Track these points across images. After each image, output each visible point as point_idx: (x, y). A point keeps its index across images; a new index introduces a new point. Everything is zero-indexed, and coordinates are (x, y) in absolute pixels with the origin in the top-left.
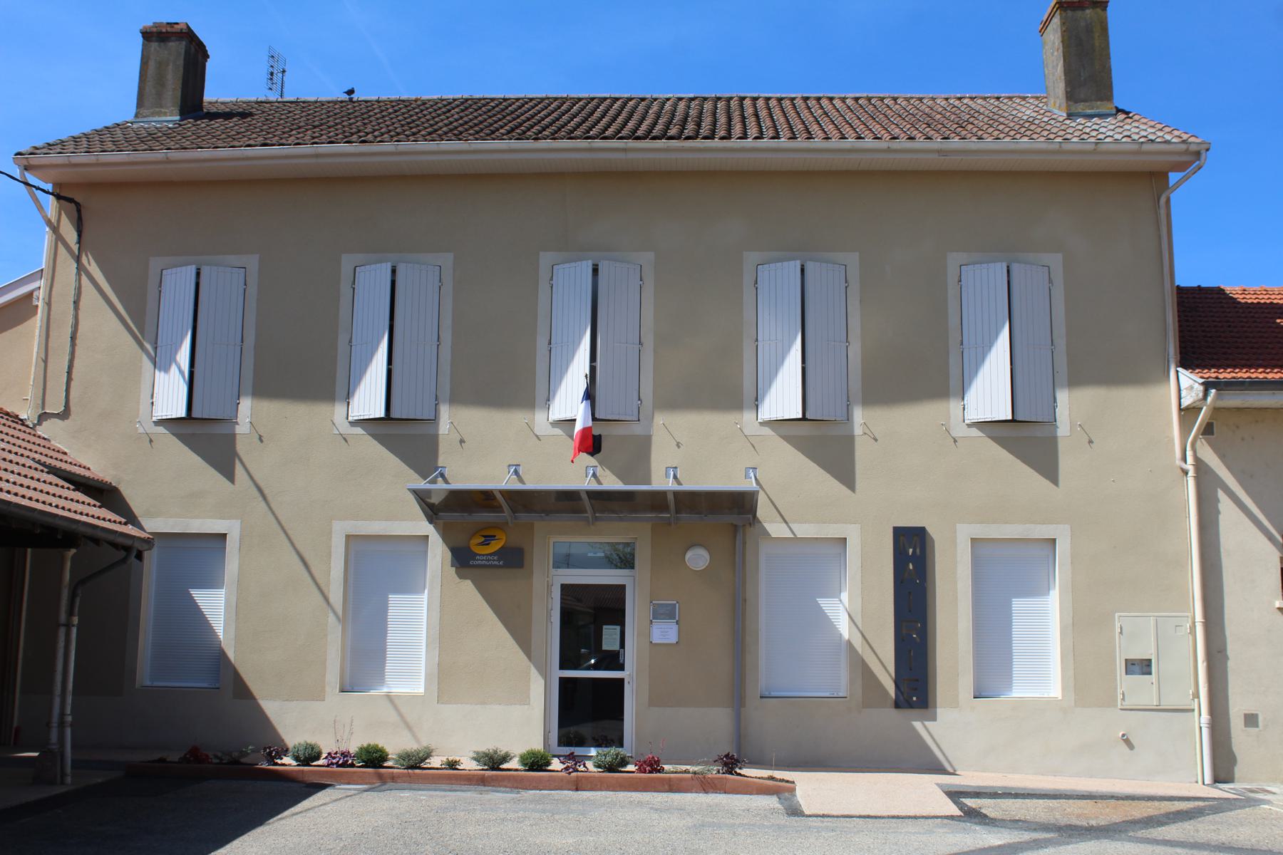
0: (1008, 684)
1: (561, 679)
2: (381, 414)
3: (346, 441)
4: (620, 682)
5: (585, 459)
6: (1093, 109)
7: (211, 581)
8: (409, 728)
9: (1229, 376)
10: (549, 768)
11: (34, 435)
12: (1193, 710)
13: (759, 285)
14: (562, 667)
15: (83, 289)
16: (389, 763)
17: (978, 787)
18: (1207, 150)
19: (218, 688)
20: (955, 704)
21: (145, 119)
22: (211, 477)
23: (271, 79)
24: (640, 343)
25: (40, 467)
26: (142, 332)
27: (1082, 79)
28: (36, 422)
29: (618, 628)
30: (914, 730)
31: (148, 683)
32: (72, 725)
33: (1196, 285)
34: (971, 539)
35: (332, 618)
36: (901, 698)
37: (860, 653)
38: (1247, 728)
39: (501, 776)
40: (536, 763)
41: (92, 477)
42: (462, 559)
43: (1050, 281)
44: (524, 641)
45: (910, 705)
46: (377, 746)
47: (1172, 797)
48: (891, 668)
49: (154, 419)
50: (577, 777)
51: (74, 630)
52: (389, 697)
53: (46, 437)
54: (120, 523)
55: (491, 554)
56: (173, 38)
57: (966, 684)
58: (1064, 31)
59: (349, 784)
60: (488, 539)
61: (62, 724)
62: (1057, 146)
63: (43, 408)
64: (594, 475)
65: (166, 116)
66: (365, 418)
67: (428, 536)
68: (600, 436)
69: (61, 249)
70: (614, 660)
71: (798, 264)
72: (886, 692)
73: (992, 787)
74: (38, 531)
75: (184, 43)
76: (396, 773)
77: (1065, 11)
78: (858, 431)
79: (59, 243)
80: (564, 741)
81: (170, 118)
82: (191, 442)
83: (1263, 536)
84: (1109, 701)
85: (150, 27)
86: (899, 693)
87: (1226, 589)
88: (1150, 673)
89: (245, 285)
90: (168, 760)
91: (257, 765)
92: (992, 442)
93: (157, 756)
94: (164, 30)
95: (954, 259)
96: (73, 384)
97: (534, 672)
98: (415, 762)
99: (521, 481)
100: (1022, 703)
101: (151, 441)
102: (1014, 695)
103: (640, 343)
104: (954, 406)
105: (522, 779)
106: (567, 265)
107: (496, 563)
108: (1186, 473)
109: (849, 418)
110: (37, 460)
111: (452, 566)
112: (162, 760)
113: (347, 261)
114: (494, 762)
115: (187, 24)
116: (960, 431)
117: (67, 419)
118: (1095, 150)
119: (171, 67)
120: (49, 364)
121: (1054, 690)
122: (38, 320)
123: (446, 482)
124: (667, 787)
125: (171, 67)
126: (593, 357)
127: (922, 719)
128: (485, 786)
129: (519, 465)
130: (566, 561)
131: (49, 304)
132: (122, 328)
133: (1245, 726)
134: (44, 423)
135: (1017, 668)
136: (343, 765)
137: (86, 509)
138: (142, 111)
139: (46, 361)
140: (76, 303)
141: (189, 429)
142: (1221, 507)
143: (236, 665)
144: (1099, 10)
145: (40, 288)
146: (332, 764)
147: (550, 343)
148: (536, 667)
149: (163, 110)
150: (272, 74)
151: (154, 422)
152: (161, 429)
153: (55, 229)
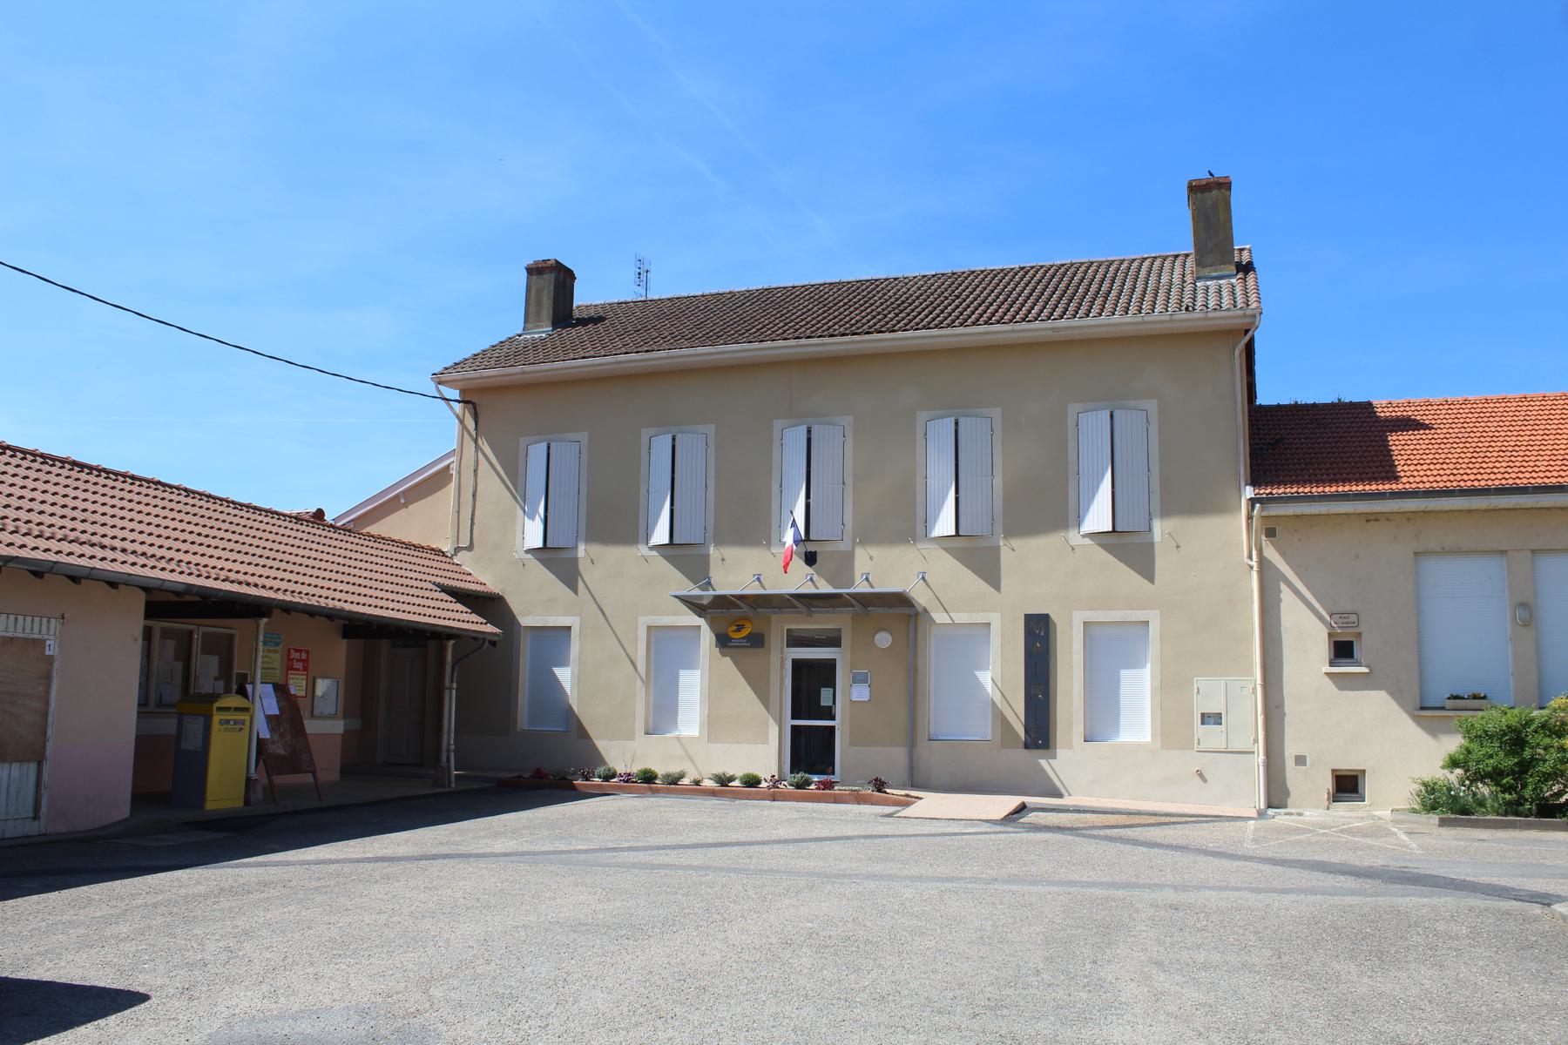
0: (1117, 734)
1: (792, 726)
2: (667, 541)
4: (833, 728)
7: (563, 663)
8: (691, 760)
10: (760, 786)
12: (1254, 752)
14: (793, 718)
16: (657, 782)
17: (1057, 805)
18: (1261, 313)
20: (1070, 746)
22: (561, 589)
24: (844, 483)
25: (435, 588)
26: (517, 492)
29: (832, 690)
30: (1039, 764)
31: (526, 728)
34: (1084, 623)
35: (639, 683)
36: (1029, 741)
37: (1000, 706)
41: (486, 591)
42: (723, 641)
43: (1148, 422)
44: (765, 701)
45: (1037, 747)
51: (454, 692)
52: (678, 738)
54: (481, 623)
57: (1078, 731)
61: (448, 750)
62: (1140, 319)
64: (811, 579)
65: (543, 327)
68: (816, 552)
70: (829, 713)
71: (953, 419)
72: (1018, 735)
73: (1067, 805)
75: (553, 274)
81: (543, 331)
82: (546, 563)
84: (1187, 743)
86: (1028, 738)
87: (1284, 659)
88: (1221, 724)
93: (516, 775)
95: (1073, 408)
96: (475, 526)
97: (771, 720)
98: (674, 780)
99: (763, 586)
101: (524, 565)
103: (844, 483)
105: (739, 792)
106: (791, 429)
108: (1252, 567)
112: (520, 777)
113: (645, 433)
114: (724, 781)
115: (556, 261)
119: (546, 292)
121: (1146, 737)
122: (453, 486)
125: (546, 292)
126: (808, 496)
127: (1047, 758)
130: (795, 640)
131: (459, 473)
133: (1296, 764)
134: (459, 554)
136: (627, 782)
138: (530, 326)
139: (458, 512)
142: (1282, 596)
147: (781, 486)
150: (640, 274)
152: (529, 556)
153: (461, 422)
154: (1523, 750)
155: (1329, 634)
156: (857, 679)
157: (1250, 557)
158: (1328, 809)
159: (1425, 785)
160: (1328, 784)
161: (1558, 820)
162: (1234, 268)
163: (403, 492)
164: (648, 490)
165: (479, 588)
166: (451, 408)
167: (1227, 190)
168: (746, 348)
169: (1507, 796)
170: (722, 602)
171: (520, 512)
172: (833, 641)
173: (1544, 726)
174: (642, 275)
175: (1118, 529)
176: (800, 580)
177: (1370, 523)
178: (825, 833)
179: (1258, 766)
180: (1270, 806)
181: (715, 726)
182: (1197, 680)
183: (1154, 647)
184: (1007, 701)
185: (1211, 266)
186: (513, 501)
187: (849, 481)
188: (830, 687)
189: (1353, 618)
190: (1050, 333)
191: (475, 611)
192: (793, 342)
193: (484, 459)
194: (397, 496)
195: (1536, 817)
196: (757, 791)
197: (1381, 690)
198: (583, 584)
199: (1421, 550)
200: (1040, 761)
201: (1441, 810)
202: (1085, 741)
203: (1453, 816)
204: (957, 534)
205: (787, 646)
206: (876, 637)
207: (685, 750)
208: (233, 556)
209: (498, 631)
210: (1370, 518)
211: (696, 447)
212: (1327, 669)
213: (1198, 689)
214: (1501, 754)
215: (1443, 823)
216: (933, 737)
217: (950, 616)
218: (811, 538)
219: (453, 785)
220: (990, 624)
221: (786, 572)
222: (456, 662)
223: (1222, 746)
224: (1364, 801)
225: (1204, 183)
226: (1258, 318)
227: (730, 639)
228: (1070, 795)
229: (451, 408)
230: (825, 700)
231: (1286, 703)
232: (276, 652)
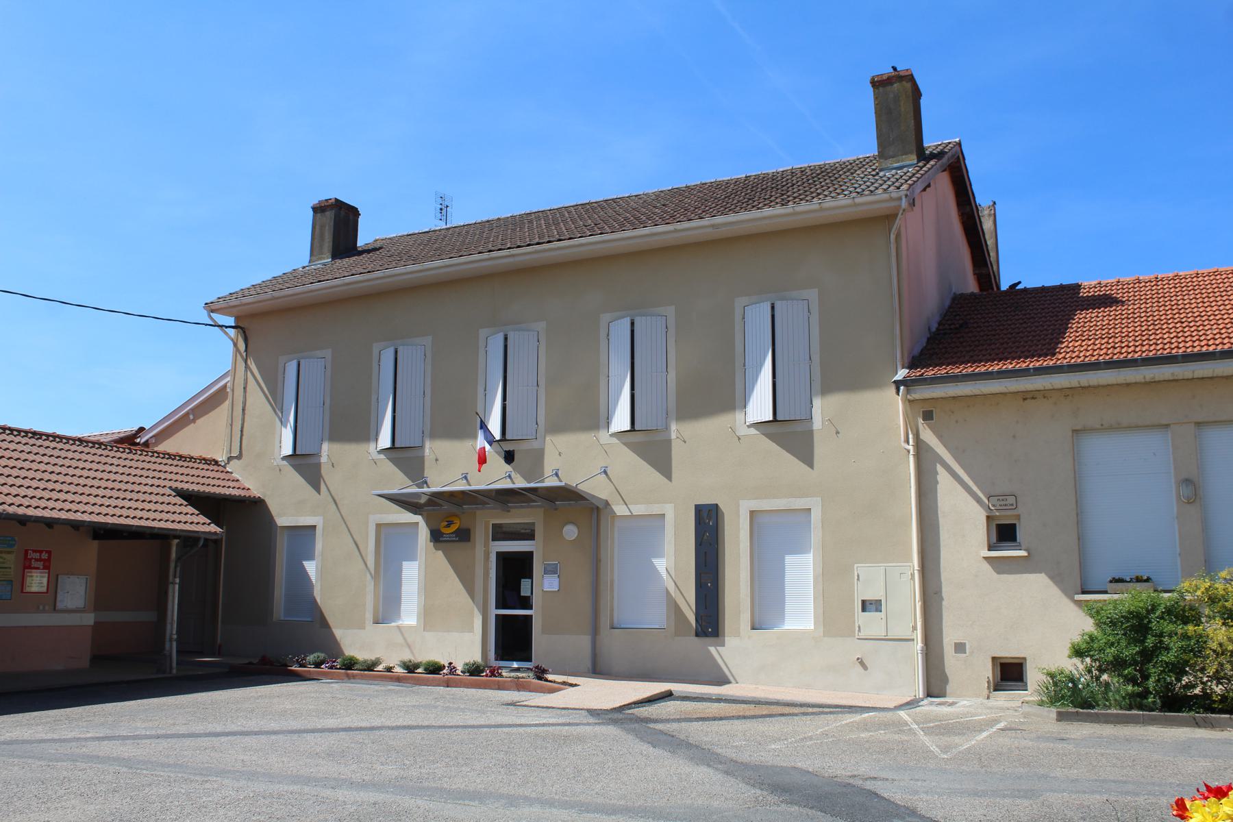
4: (529, 618)
6: (899, 162)
8: (409, 647)
9: (1038, 364)
12: (913, 640)
17: (701, 694)
20: (737, 634)
21: (314, 263)
23: (441, 213)
26: (276, 405)
27: (891, 139)
29: (530, 580)
30: (709, 652)
31: (282, 618)
33: (1059, 284)
35: (368, 576)
36: (700, 629)
40: (474, 670)
42: (436, 536)
44: (471, 591)
47: (822, 705)
48: (694, 608)
51: (177, 586)
55: (452, 533)
58: (877, 104)
60: (450, 524)
64: (510, 476)
65: (324, 259)
66: (384, 448)
68: (514, 450)
74: (102, 532)
77: (877, 88)
78: (673, 436)
82: (297, 468)
83: (972, 499)
84: (849, 630)
87: (942, 543)
88: (881, 611)
91: (291, 667)
92: (765, 438)
93: (247, 662)
95: (740, 302)
96: (244, 437)
97: (476, 611)
98: (370, 667)
100: (789, 632)
101: (280, 470)
104: (739, 416)
105: (423, 679)
107: (454, 539)
109: (667, 428)
110: (173, 488)
112: (250, 663)
113: (376, 348)
114: (411, 668)
116: (743, 431)
118: (821, 208)
119: (327, 228)
122: (227, 403)
124: (497, 687)
125: (327, 228)
127: (716, 645)
129: (467, 474)
130: (501, 533)
133: (956, 653)
134: (231, 463)
137: (189, 518)
139: (231, 425)
140: (245, 388)
141: (394, 454)
142: (939, 478)
147: (485, 390)
150: (441, 209)
153: (235, 345)
154: (1145, 638)
155: (988, 517)
157: (908, 443)
158: (988, 698)
159: (1052, 676)
160: (987, 672)
161: (1184, 714)
163: (192, 410)
164: (378, 399)
168: (447, 263)
169: (1130, 688)
171: (278, 423)
172: (530, 536)
173: (1169, 611)
174: (443, 210)
176: (498, 475)
177: (1026, 401)
178: (400, 722)
179: (917, 653)
181: (429, 616)
183: (816, 535)
185: (893, 157)
187: (542, 383)
188: (529, 578)
189: (1011, 500)
190: (710, 230)
192: (486, 255)
194: (187, 414)
195: (1161, 711)
196: (390, 675)
197: (1041, 573)
198: (325, 487)
204: (633, 429)
205: (492, 540)
206: (564, 529)
207: (405, 639)
208: (127, 471)
209: (219, 530)
210: (1027, 396)
211: (415, 357)
213: (858, 576)
214: (1123, 643)
215: (1061, 717)
217: (628, 508)
219: (174, 671)
221: (479, 471)
223: (882, 634)
225: (884, 78)
228: (737, 683)
229: (226, 333)
230: (525, 592)
231: (944, 589)
232: (9, 553)
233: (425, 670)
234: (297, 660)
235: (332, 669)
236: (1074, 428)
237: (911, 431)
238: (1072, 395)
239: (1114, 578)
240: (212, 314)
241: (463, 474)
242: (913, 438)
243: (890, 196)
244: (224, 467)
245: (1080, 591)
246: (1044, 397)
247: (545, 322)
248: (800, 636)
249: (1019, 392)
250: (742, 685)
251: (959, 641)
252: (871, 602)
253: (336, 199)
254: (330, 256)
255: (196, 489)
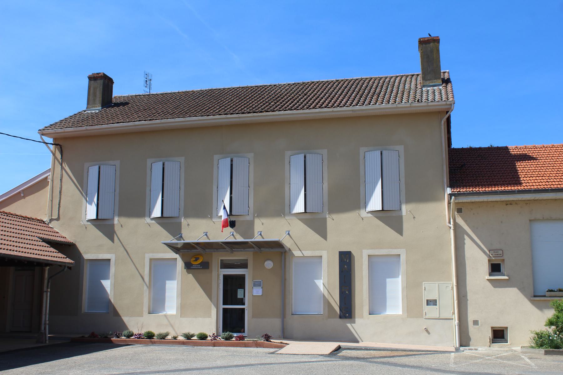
1: (224, 309)
3: (150, 226)
4: (243, 310)
5: (229, 229)
6: (433, 83)
7: (106, 278)
8: (172, 326)
10: (207, 339)
11: (49, 227)
12: (453, 319)
13: (291, 163)
14: (224, 304)
15: (63, 175)
16: (154, 338)
17: (356, 346)
18: (454, 103)
19: (108, 313)
20: (362, 317)
21: (90, 109)
22: (105, 240)
23: (146, 83)
24: (249, 187)
25: (39, 240)
26: (82, 190)
27: (429, 71)
28: (49, 222)
29: (243, 290)
31: (87, 311)
32: (48, 324)
34: (368, 255)
35: (145, 288)
38: (474, 326)
39: (189, 341)
41: (66, 241)
42: (188, 266)
43: (399, 156)
44: (209, 296)
46: (149, 331)
48: (338, 303)
49: (87, 220)
50: (214, 342)
51: (49, 293)
52: (166, 316)
53: (52, 227)
54: (64, 258)
56: (99, 79)
58: (422, 53)
59: (140, 344)
60: (197, 259)
61: (45, 324)
63: (51, 217)
64: (233, 235)
65: (97, 107)
66: (155, 217)
67: (177, 258)
68: (235, 221)
69: (56, 161)
70: (242, 302)
71: (303, 155)
72: (336, 312)
74: (26, 263)
76: (156, 341)
77: (422, 45)
79: (56, 160)
80: (224, 330)
81: (97, 109)
82: (98, 227)
83: (481, 252)
84: (420, 315)
85: (92, 75)
86: (341, 313)
88: (436, 305)
89: (116, 171)
90: (85, 337)
93: (81, 336)
94: (95, 76)
95: (362, 150)
96: (61, 208)
97: (213, 306)
98: (163, 337)
99: (208, 238)
100: (388, 316)
101: (86, 228)
102: (387, 313)
103: (249, 187)
106: (223, 159)
108: (450, 228)
111: (185, 269)
112: (83, 337)
113: (149, 161)
114: (189, 337)
115: (103, 73)
117: (59, 220)
120: (53, 202)
121: (399, 311)
122: (49, 188)
123: (184, 240)
124: (244, 345)
125: (98, 89)
127: (351, 323)
128: (184, 345)
130: (225, 265)
131: (53, 181)
132: (76, 188)
133: (474, 325)
135: (388, 304)
136: (139, 338)
138: (90, 106)
139: (52, 201)
140: (61, 180)
142: (466, 241)
143: (114, 305)
144: (436, 43)
145: (50, 175)
146: (136, 338)
147: (218, 188)
148: (213, 304)
149: (96, 105)
150: (146, 81)
151: (87, 221)
152: (89, 223)
153: (54, 154)
155: (489, 261)
156: (256, 284)
157: (450, 223)
159: (537, 334)
160: (490, 334)
162: (441, 81)
163: (23, 190)
164: (150, 190)
165: (62, 240)
166: (49, 148)
167: (437, 43)
170: (188, 246)
171: (84, 201)
172: (244, 265)
174: (148, 82)
175: (385, 209)
177: (507, 206)
178: (240, 363)
179: (455, 326)
180: (461, 345)
181: (183, 309)
182: (424, 283)
184: (331, 296)
186: (81, 195)
188: (243, 289)
189: (500, 252)
190: (351, 112)
191: (60, 251)
193: (66, 173)
194: (19, 193)
196: (205, 342)
199: (533, 219)
200: (347, 324)
201: (545, 347)
202: (369, 314)
203: (552, 350)
204: (305, 212)
207: (169, 322)
209: (72, 261)
212: (488, 277)
213: (425, 288)
215: (547, 353)
216: (293, 313)
217: (302, 252)
218: (233, 214)
219: (47, 342)
220: (322, 256)
222: (50, 277)
223: (437, 316)
224: (507, 343)
225: (426, 39)
226: (453, 106)
227: (192, 265)
229: (49, 148)
230: (240, 295)
233: (198, 338)
234: (116, 334)
235: (140, 339)
236: (530, 219)
237: (452, 218)
238: (530, 203)
239: (549, 290)
240: (42, 136)
241: (204, 233)
242: (453, 221)
243: (446, 103)
244: (48, 224)
245: (533, 295)
246: (516, 204)
247: (253, 154)
248: (394, 318)
249: (504, 201)
250: (365, 342)
251: (475, 320)
252: (431, 301)
253: (104, 73)
254: (101, 106)
255: (62, 240)
